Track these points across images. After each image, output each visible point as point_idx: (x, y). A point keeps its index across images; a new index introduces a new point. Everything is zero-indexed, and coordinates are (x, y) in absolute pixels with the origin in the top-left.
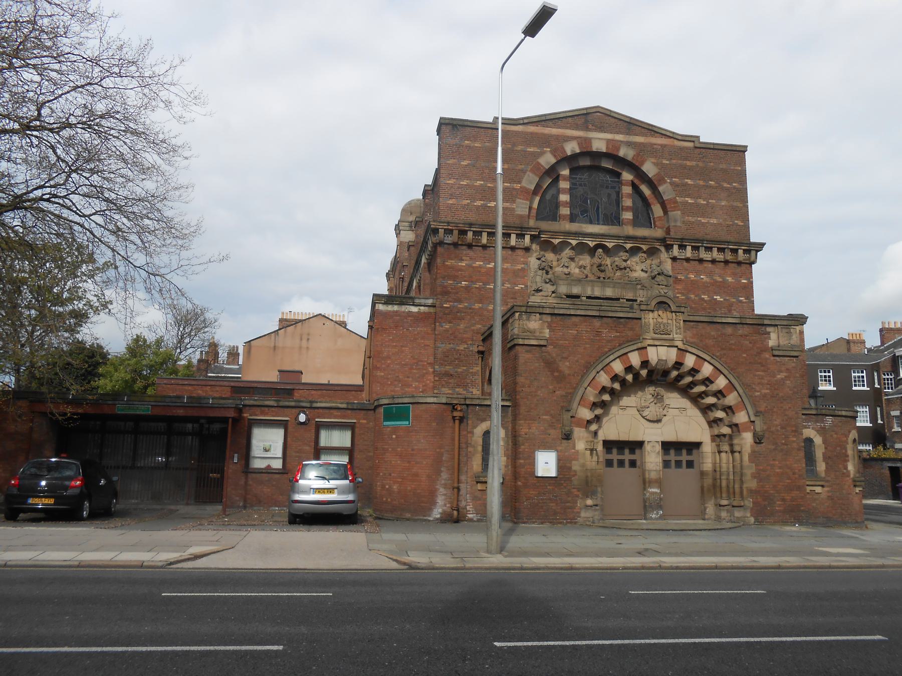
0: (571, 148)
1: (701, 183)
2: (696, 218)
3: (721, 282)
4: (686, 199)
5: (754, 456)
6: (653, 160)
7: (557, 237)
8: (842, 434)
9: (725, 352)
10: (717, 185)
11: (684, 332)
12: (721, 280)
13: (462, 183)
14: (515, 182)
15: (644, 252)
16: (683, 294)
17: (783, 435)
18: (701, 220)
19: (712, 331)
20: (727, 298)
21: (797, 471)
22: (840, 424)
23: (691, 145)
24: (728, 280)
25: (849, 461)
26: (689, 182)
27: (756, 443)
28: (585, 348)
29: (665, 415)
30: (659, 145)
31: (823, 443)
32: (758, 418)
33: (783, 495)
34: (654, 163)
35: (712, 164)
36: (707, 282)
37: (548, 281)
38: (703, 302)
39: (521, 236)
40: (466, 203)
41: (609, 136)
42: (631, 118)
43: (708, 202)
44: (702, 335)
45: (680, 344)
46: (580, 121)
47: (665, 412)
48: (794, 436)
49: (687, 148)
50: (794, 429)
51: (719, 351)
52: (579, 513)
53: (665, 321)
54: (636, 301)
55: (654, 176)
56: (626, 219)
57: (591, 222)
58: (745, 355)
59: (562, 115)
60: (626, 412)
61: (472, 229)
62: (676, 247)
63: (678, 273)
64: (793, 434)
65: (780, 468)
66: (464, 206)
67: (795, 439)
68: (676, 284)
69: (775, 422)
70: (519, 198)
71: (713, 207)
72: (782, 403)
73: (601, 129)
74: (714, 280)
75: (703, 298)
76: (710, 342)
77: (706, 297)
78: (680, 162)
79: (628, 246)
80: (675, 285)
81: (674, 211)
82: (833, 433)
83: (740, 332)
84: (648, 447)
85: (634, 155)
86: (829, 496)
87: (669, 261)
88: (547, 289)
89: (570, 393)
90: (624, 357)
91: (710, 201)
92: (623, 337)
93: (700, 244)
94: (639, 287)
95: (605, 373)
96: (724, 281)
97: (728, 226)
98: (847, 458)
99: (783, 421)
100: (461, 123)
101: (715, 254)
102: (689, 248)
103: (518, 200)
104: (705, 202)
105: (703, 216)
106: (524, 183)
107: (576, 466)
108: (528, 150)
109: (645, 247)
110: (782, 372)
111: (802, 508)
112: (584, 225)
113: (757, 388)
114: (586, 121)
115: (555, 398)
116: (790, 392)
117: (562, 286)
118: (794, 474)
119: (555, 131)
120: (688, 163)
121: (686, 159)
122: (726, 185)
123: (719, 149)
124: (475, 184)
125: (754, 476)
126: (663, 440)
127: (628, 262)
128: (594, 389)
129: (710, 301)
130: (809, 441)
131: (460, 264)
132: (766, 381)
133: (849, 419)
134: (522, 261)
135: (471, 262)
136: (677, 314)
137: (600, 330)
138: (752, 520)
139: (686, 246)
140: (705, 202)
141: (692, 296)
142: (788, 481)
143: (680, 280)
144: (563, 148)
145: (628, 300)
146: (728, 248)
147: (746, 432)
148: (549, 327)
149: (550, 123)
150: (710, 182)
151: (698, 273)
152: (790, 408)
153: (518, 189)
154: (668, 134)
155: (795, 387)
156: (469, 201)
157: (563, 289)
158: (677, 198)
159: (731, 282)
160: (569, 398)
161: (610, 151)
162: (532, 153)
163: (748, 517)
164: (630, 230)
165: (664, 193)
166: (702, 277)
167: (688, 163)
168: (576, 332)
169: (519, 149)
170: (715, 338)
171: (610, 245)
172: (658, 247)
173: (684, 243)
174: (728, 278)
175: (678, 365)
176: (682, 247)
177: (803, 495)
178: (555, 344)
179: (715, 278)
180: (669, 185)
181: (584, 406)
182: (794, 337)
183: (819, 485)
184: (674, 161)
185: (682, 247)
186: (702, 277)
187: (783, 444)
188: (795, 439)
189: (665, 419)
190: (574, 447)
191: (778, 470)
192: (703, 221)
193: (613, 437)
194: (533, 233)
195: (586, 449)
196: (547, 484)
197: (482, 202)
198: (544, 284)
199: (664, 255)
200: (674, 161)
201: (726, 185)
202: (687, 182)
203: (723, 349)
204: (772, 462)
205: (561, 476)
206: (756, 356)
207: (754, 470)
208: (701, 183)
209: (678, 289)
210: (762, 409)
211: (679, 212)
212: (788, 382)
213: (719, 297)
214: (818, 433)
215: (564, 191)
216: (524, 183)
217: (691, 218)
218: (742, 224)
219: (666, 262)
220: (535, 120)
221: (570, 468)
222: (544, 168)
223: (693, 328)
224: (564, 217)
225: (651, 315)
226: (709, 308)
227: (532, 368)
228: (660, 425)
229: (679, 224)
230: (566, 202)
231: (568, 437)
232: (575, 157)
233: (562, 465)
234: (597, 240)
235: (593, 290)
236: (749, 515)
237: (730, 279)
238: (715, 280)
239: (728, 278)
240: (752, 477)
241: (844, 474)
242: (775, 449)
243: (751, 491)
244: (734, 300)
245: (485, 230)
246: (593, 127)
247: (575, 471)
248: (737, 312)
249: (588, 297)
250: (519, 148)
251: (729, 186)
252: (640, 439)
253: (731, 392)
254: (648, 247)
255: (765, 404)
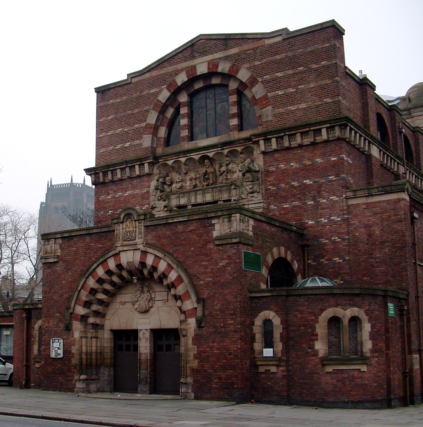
0: (181, 79)
1: (290, 72)
2: (285, 108)
3: (310, 165)
4: (277, 92)
5: (197, 339)
6: (247, 65)
7: (170, 159)
8: (310, 313)
9: (177, 248)
10: (306, 69)
11: (146, 236)
12: (310, 163)
13: (108, 134)
14: (142, 122)
15: (241, 153)
16: (273, 185)
17: (222, 318)
18: (290, 109)
19: (166, 232)
20: (317, 180)
21: (233, 351)
22: (306, 303)
23: (279, 39)
24: (317, 162)
25: (317, 340)
26: (279, 75)
27: (198, 327)
28: (81, 260)
29: (152, 307)
30: (251, 49)
31: (281, 324)
32: (200, 305)
33: (219, 373)
34: (248, 68)
35: (300, 50)
36: (296, 168)
37: (160, 198)
38: (293, 189)
39: (142, 165)
40: (111, 149)
41: (209, 58)
42: (226, 35)
43: (297, 89)
44: (159, 236)
45: (141, 247)
46: (187, 54)
47: (151, 305)
48: (232, 319)
49: (276, 43)
50: (232, 312)
51: (172, 248)
52: (75, 384)
53: (131, 229)
54: (230, 200)
55: (248, 80)
56: (232, 126)
57: (208, 137)
58: (193, 249)
59: (174, 54)
60: (125, 307)
61: (110, 169)
62: (262, 143)
63: (270, 166)
64: (231, 317)
65: (218, 349)
66: (109, 152)
67: (232, 322)
68: (268, 176)
69: (216, 307)
70: (146, 134)
71: (302, 91)
72: (222, 288)
73: (204, 53)
74: (303, 165)
75: (293, 185)
76: (164, 241)
77: (295, 184)
78: (270, 58)
79: (226, 152)
80: (266, 178)
81: (266, 107)
82: (296, 313)
83: (190, 228)
84: (140, 335)
85: (231, 67)
86: (284, 376)
87: (261, 157)
88: (160, 205)
89: (72, 295)
90: (105, 264)
91: (299, 87)
92: (104, 247)
93: (282, 134)
94: (233, 187)
95: (93, 277)
96: (313, 164)
97: (317, 107)
98: (314, 338)
99: (222, 305)
100: (107, 88)
101: (298, 140)
102: (274, 140)
103: (145, 136)
104: (294, 90)
105: (292, 104)
106: (148, 121)
107: (74, 350)
108: (151, 92)
109: (239, 149)
110: (223, 259)
111: (236, 386)
112: (199, 141)
113: (202, 278)
114: (193, 51)
115: (62, 300)
116: (231, 278)
117: (173, 200)
118: (230, 354)
119: (169, 69)
120: (278, 57)
121: (276, 54)
122: (314, 66)
123: (306, 33)
124: (117, 132)
125: (195, 357)
126: (150, 328)
127: (230, 166)
128: (85, 291)
129: (300, 186)
130: (267, 322)
131: (107, 198)
132: (209, 270)
133: (322, 297)
134: (147, 185)
135: (114, 194)
136: (140, 221)
137: (90, 245)
138: (193, 395)
139: (270, 139)
140: (294, 90)
141: (283, 185)
142: (224, 361)
143: (273, 172)
144: (175, 81)
145: (224, 201)
146: (311, 130)
147: (191, 317)
148: (61, 247)
149: (166, 64)
150: (299, 69)
151: (288, 161)
152: (229, 292)
153: (145, 127)
154: (259, 36)
155: (234, 273)
156: (113, 147)
157: (174, 202)
158: (268, 94)
159: (321, 163)
160: (69, 299)
161: (211, 71)
162: (153, 94)
163: (189, 393)
164: (236, 135)
165: (256, 93)
166: (292, 164)
167: (278, 57)
168: (75, 249)
169: (145, 93)
170: (169, 237)
171: (211, 155)
172: (251, 145)
173: (269, 137)
174: (317, 160)
175: (143, 264)
176: (267, 141)
177: (237, 374)
178: (63, 260)
179: (304, 162)
180: (260, 84)
181: (80, 305)
182: (235, 224)
183: (272, 365)
184: (265, 61)
185: (267, 141)
186: (292, 164)
187: (221, 327)
188: (232, 322)
189: (152, 310)
190: (73, 336)
191: (215, 352)
192: (292, 109)
193: (116, 327)
194: (149, 161)
195: (81, 337)
196: (57, 363)
197: (121, 145)
198: (156, 202)
199: (257, 153)
200: (265, 61)
201: (314, 66)
202: (277, 76)
203: (176, 246)
204: (211, 344)
205: (65, 358)
206: (201, 247)
207: (196, 352)
208: (290, 72)
209: (269, 181)
210: (205, 296)
211: (270, 107)
212: (229, 268)
213: (308, 181)
214: (277, 314)
215: (183, 116)
216: (148, 121)
217: (280, 109)
218: (331, 100)
219: (258, 158)
220: (154, 65)
221: (70, 352)
222: (162, 103)
223: (153, 231)
224: (183, 139)
225: (121, 225)
226: (299, 194)
227: (51, 279)
228: (147, 315)
229: (270, 118)
230: (185, 125)
231: (68, 328)
232: (186, 86)
233: (66, 351)
234: (201, 152)
235: (196, 198)
236: (190, 391)
237: (319, 160)
238: (305, 164)
239: (317, 160)
240: (194, 358)
241: (308, 353)
242: (214, 332)
243: (192, 370)
244: (324, 181)
245: (118, 167)
246: (198, 55)
247: (73, 354)
248: (327, 192)
249: (193, 205)
250: (145, 92)
251: (317, 66)
252: (135, 328)
253: (180, 283)
254: (242, 147)
255: (208, 291)
